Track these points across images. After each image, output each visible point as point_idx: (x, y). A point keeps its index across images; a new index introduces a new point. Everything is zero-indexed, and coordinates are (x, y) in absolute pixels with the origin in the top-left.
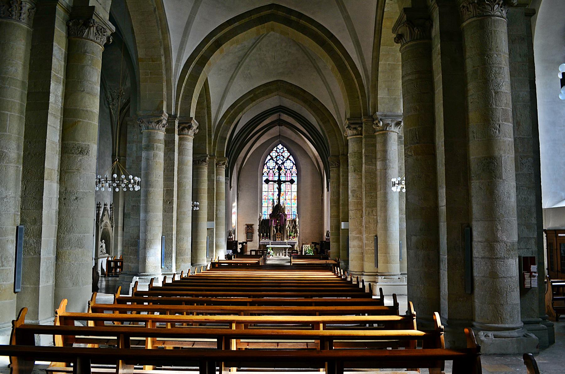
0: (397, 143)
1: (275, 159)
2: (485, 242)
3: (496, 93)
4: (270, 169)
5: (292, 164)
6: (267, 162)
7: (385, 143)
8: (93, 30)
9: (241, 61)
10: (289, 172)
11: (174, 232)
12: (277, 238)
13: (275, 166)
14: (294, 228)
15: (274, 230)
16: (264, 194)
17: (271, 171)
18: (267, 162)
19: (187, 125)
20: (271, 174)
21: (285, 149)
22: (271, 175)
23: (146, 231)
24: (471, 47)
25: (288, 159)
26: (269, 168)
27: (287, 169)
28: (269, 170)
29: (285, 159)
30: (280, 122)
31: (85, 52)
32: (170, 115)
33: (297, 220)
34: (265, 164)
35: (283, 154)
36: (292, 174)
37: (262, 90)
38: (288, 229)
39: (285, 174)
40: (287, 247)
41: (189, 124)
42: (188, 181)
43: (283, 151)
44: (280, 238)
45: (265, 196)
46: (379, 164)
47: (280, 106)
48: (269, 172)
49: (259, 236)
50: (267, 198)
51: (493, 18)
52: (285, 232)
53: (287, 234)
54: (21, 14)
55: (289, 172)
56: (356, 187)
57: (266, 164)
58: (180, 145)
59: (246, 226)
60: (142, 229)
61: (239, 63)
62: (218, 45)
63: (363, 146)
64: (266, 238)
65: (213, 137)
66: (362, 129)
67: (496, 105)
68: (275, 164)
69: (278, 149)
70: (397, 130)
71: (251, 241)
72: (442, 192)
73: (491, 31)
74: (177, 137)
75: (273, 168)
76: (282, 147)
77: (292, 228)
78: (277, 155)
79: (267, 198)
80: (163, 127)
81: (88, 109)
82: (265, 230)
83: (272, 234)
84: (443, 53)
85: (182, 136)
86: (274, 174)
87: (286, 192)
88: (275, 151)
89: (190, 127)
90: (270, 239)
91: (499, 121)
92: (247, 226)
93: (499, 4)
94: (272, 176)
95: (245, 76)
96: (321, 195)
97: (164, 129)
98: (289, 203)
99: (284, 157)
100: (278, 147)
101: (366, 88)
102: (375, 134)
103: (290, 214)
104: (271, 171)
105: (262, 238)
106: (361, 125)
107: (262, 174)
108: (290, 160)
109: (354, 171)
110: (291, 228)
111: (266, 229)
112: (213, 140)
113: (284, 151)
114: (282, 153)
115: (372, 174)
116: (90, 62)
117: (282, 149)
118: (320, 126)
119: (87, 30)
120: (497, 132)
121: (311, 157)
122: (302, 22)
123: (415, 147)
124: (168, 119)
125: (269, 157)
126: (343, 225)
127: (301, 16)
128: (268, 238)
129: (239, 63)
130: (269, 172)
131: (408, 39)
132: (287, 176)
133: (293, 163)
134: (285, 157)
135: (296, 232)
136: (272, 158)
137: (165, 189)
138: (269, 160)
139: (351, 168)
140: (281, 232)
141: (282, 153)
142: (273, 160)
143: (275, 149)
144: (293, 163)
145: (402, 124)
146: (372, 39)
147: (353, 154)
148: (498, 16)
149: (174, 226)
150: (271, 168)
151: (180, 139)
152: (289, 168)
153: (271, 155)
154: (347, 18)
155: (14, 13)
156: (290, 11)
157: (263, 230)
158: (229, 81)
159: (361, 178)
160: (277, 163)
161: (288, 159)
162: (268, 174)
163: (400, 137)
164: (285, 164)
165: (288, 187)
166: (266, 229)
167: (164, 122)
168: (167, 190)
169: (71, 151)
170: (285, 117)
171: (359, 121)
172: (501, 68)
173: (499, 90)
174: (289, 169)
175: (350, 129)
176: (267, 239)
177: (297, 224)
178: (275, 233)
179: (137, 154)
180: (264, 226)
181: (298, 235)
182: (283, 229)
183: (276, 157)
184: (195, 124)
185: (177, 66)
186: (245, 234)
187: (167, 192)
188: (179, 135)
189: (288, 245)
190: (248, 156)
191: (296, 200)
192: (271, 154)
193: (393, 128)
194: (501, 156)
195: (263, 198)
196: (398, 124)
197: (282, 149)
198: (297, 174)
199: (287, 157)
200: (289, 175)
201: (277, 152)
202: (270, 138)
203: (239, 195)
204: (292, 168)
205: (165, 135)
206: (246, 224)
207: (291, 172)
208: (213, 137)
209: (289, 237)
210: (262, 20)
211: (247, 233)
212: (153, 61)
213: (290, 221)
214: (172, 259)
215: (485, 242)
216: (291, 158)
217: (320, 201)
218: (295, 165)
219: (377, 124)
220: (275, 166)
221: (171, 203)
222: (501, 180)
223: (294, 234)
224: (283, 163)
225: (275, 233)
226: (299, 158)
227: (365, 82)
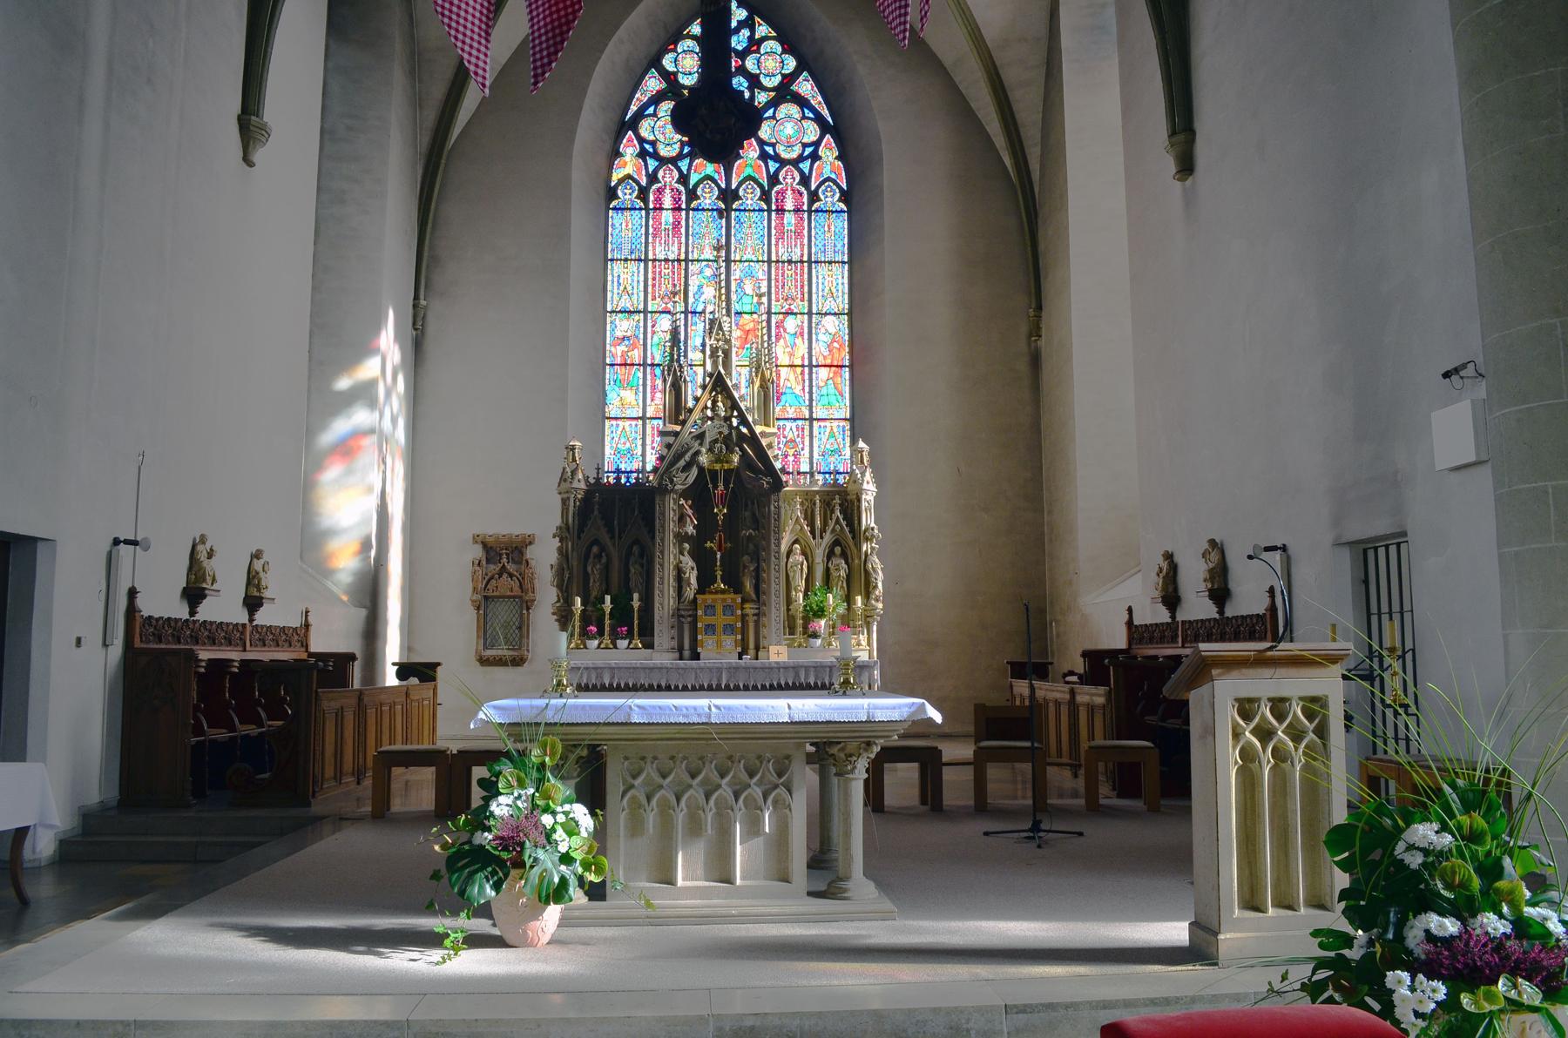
5: (812, 132)
10: (790, 178)
12: (711, 629)
14: (844, 555)
15: (679, 572)
16: (622, 326)
17: (668, 177)
18: (640, 115)
20: (668, 191)
21: (762, 30)
22: (667, 202)
25: (784, 93)
26: (656, 156)
27: (777, 158)
28: (652, 164)
35: (750, 64)
36: (814, 197)
38: (801, 558)
39: (765, 196)
40: (863, 733)
43: (751, 39)
44: (729, 629)
45: (622, 348)
48: (653, 178)
49: (564, 618)
50: (636, 356)
52: (775, 588)
53: (789, 601)
55: (790, 178)
57: (634, 124)
59: (478, 552)
64: (615, 636)
71: (518, 662)
77: (830, 555)
79: (636, 356)
82: (607, 569)
83: (665, 602)
86: (692, 195)
87: (774, 319)
90: (649, 645)
92: (485, 545)
94: (677, 209)
96: (1024, 328)
98: (798, 389)
103: (805, 467)
105: (585, 634)
107: (602, 192)
108: (802, 102)
110: (819, 555)
111: (616, 563)
113: (754, 44)
117: (745, 33)
121: (947, 59)
125: (653, 84)
128: (630, 636)
130: (653, 178)
132: (781, 211)
133: (819, 119)
134: (765, 82)
135: (858, 581)
140: (735, 585)
150: (664, 151)
152: (794, 155)
153: (670, 67)
157: (595, 571)
161: (784, 93)
162: (643, 194)
165: (790, 284)
166: (616, 563)
174: (795, 163)
176: (622, 644)
177: (868, 520)
178: (690, 593)
180: (605, 538)
181: (880, 605)
182: (756, 557)
186: (471, 615)
189: (892, 687)
191: (846, 373)
192: (668, 62)
195: (615, 352)
197: (745, 33)
198: (845, 197)
199: (776, 80)
200: (789, 204)
203: (431, 329)
204: (815, 157)
206: (476, 539)
207: (805, 181)
209: (806, 620)
211: (485, 601)
213: (808, 497)
216: (805, 87)
217: (1023, 366)
223: (849, 599)
225: (690, 593)
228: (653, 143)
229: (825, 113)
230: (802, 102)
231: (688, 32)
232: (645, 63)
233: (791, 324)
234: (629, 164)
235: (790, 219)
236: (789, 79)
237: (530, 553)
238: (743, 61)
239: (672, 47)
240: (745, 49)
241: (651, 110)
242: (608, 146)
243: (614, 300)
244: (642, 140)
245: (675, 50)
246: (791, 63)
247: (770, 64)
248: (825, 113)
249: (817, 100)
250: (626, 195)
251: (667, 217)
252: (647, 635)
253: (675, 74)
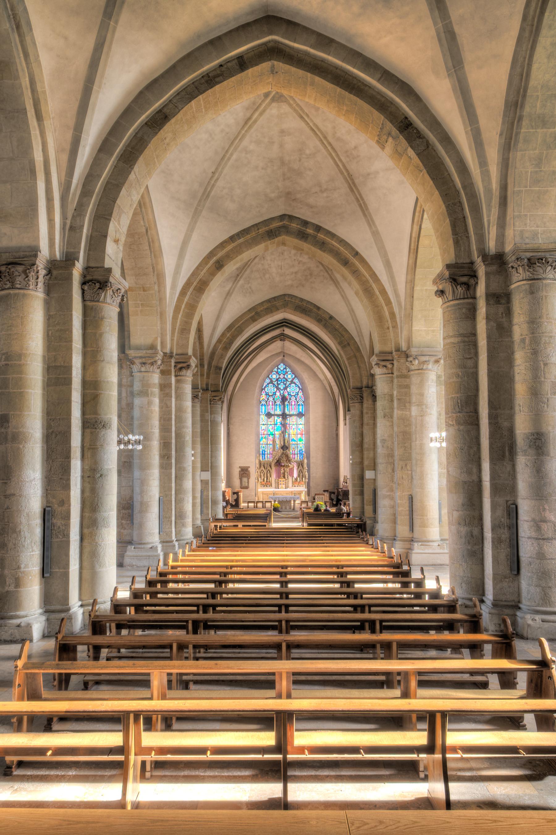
0: (435, 384)
1: (276, 383)
2: (531, 521)
3: (546, 364)
4: (270, 396)
5: (298, 389)
6: (265, 387)
7: (422, 384)
8: (110, 292)
9: (240, 273)
11: (173, 492)
18: (265, 387)
19: (184, 365)
21: (288, 370)
22: (271, 404)
23: (142, 492)
24: (519, 313)
25: (292, 382)
26: (268, 395)
28: (268, 396)
29: (288, 383)
30: (283, 337)
31: (102, 319)
32: (165, 354)
33: (306, 461)
34: (262, 389)
35: (286, 376)
36: (298, 402)
37: (265, 307)
41: (187, 364)
42: (188, 431)
46: (414, 411)
47: (285, 319)
48: (268, 399)
50: (266, 433)
51: (544, 282)
54: (37, 283)
55: (293, 399)
56: (386, 435)
57: (264, 389)
58: (177, 389)
60: (137, 489)
61: (238, 275)
62: (219, 266)
63: (395, 386)
65: (206, 367)
66: (393, 367)
67: (545, 378)
68: (275, 390)
69: (279, 370)
70: (436, 367)
72: (486, 466)
73: (542, 296)
74: (173, 379)
79: (266, 433)
80: (158, 368)
81: (109, 379)
84: (488, 318)
85: (179, 378)
86: (275, 402)
89: (188, 367)
91: (547, 394)
93: (552, 266)
95: (244, 291)
96: (335, 429)
97: (158, 371)
99: (287, 380)
100: (279, 367)
101: (398, 316)
102: (409, 373)
104: (271, 399)
106: (391, 361)
108: (296, 384)
109: (384, 417)
112: (205, 371)
113: (287, 372)
114: (284, 375)
115: (406, 421)
116: (108, 328)
118: (338, 351)
119: (103, 294)
120: (546, 406)
122: (321, 236)
123: (457, 417)
124: (163, 359)
126: (369, 475)
127: (318, 228)
129: (238, 275)
131: (450, 298)
132: (292, 405)
133: (299, 387)
136: (271, 382)
137: (162, 441)
138: (268, 384)
139: (380, 413)
142: (274, 384)
143: (276, 370)
144: (299, 387)
145: (442, 361)
146: (405, 259)
147: (383, 396)
148: (551, 279)
149: (173, 485)
150: (270, 394)
151: (178, 381)
154: (376, 234)
155: (31, 283)
156: (306, 223)
157: (262, 475)
158: (225, 298)
159: (393, 425)
160: (278, 388)
161: (292, 382)
162: (266, 402)
163: (438, 377)
164: (288, 389)
167: (159, 362)
168: (164, 443)
169: (94, 425)
170: (288, 332)
171: (390, 358)
172: (551, 337)
173: (548, 362)
174: (294, 396)
175: (379, 367)
179: (127, 401)
180: (263, 469)
183: (277, 380)
184: (193, 362)
185: (172, 294)
187: (164, 445)
188: (176, 376)
190: (241, 380)
193: (430, 366)
194: (549, 432)
195: (261, 432)
196: (437, 361)
198: (304, 402)
200: (293, 403)
202: (269, 355)
204: (298, 394)
205: (160, 378)
206: (240, 467)
207: (296, 399)
208: (206, 367)
210: (271, 234)
212: (144, 291)
214: (171, 524)
215: (531, 521)
216: (296, 381)
217: (335, 436)
218: (302, 389)
219: (411, 362)
221: (169, 457)
222: (549, 458)
224: (285, 388)
226: (306, 381)
227: (396, 310)
229: (300, 385)
230: (296, 384)
233: (294, 427)
234: (264, 396)
235: (293, 407)
236: (293, 379)
237: (249, 469)
243: (261, 423)
246: (294, 376)
247: (289, 376)
248: (300, 385)
249: (298, 383)
250: (263, 403)
251: (271, 406)
252: (271, 485)
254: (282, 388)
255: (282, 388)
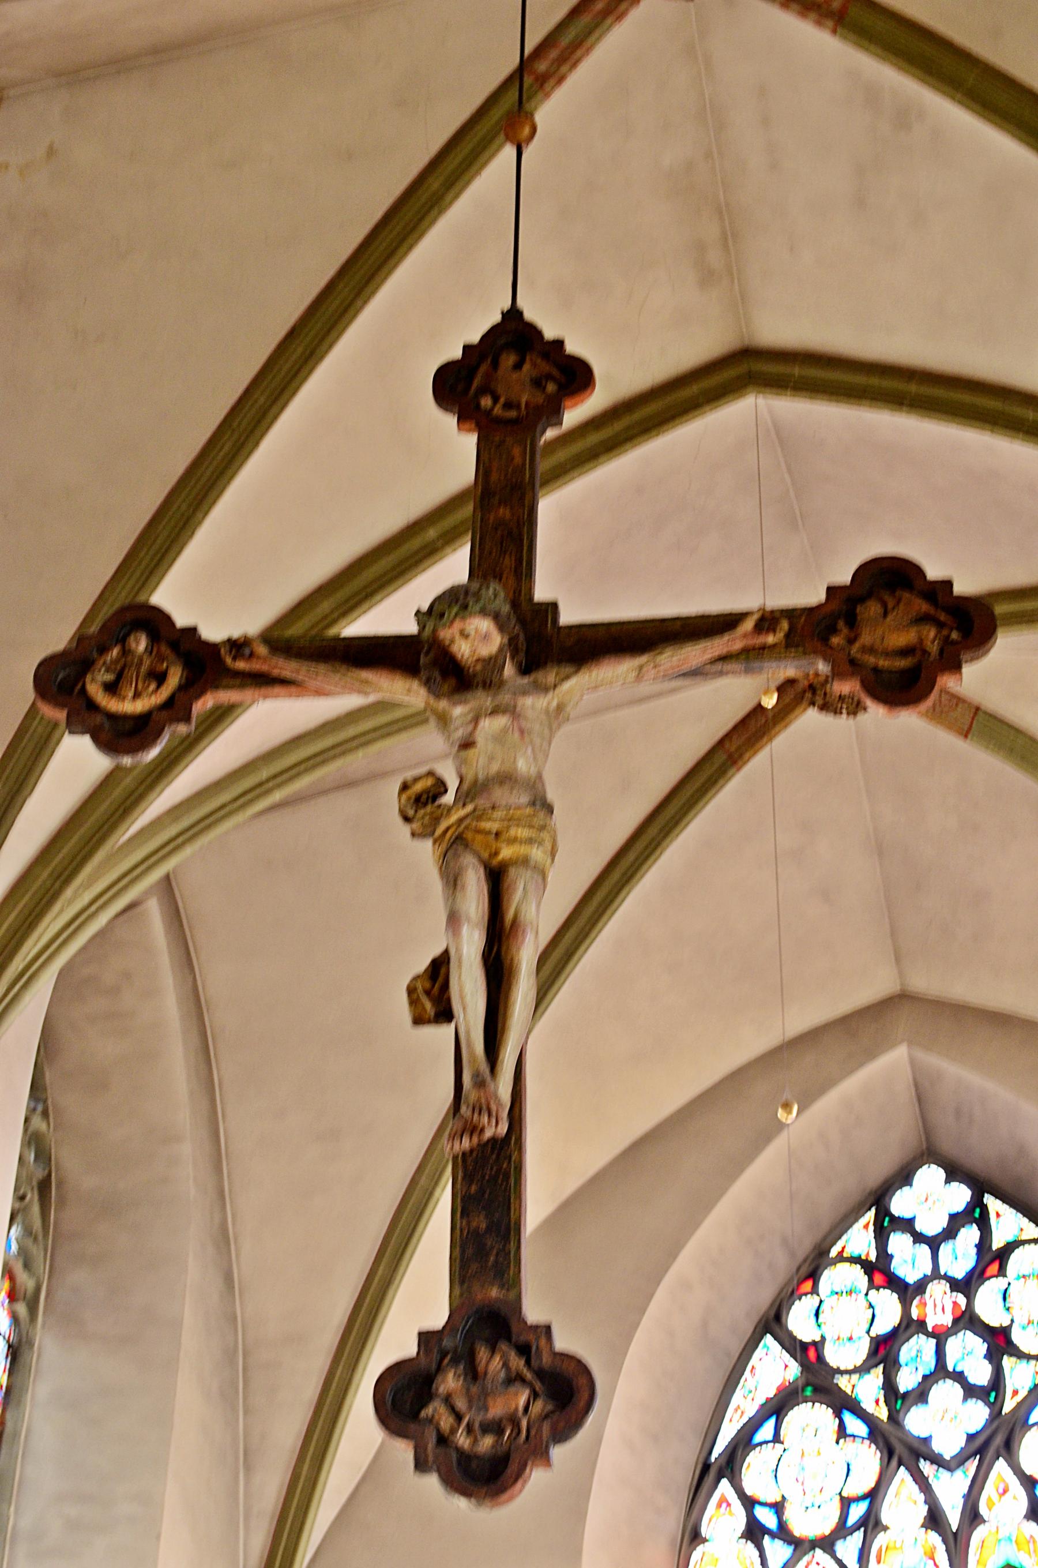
6: (744, 1442)
13: (874, 1495)
18: (744, 1442)
26: (783, 1533)
43: (983, 1245)
75: (842, 1530)
76: (960, 1195)
78: (885, 1325)
88: (857, 1276)
114: (966, 1286)
117: (970, 1234)
141: (966, 1286)
150: (803, 1526)
201: (895, 1283)
220: (874, 1495)
228: (778, 1507)
231: (841, 1253)
232: (748, 1328)
238: (970, 1298)
239: (808, 1286)
240: (970, 1274)
241: (766, 1431)
242: (673, 1521)
244: (749, 1503)
245: (815, 1291)
253: (818, 1346)
254: (948, 1445)
255: (948, 1445)
